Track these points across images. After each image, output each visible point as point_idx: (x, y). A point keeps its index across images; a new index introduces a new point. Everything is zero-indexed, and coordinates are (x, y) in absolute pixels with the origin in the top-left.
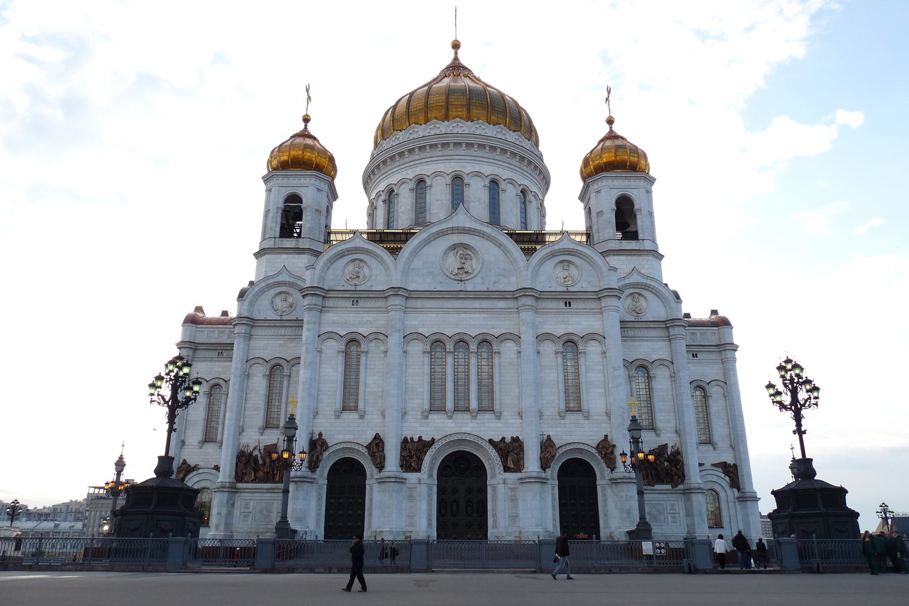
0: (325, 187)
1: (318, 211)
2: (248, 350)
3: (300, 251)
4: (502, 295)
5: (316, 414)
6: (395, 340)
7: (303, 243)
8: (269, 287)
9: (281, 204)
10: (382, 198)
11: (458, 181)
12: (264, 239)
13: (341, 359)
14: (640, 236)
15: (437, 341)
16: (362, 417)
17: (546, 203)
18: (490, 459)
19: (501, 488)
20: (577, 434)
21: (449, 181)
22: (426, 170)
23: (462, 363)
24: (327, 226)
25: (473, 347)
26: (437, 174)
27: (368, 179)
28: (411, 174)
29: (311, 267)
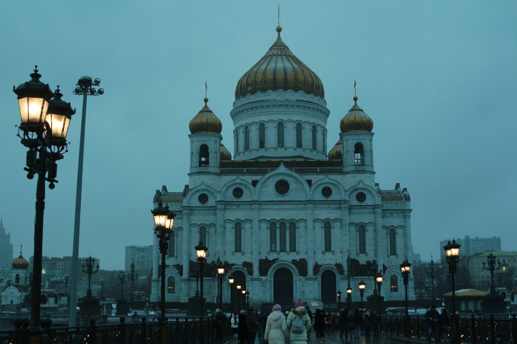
4: (300, 202)
5: (225, 253)
6: (256, 223)
7: (211, 170)
8: (197, 192)
9: (199, 150)
10: (242, 130)
12: (191, 168)
13: (234, 231)
16: (243, 255)
17: (327, 127)
18: (294, 270)
19: (298, 282)
20: (329, 260)
21: (276, 125)
23: (283, 232)
25: (288, 225)
27: (234, 115)
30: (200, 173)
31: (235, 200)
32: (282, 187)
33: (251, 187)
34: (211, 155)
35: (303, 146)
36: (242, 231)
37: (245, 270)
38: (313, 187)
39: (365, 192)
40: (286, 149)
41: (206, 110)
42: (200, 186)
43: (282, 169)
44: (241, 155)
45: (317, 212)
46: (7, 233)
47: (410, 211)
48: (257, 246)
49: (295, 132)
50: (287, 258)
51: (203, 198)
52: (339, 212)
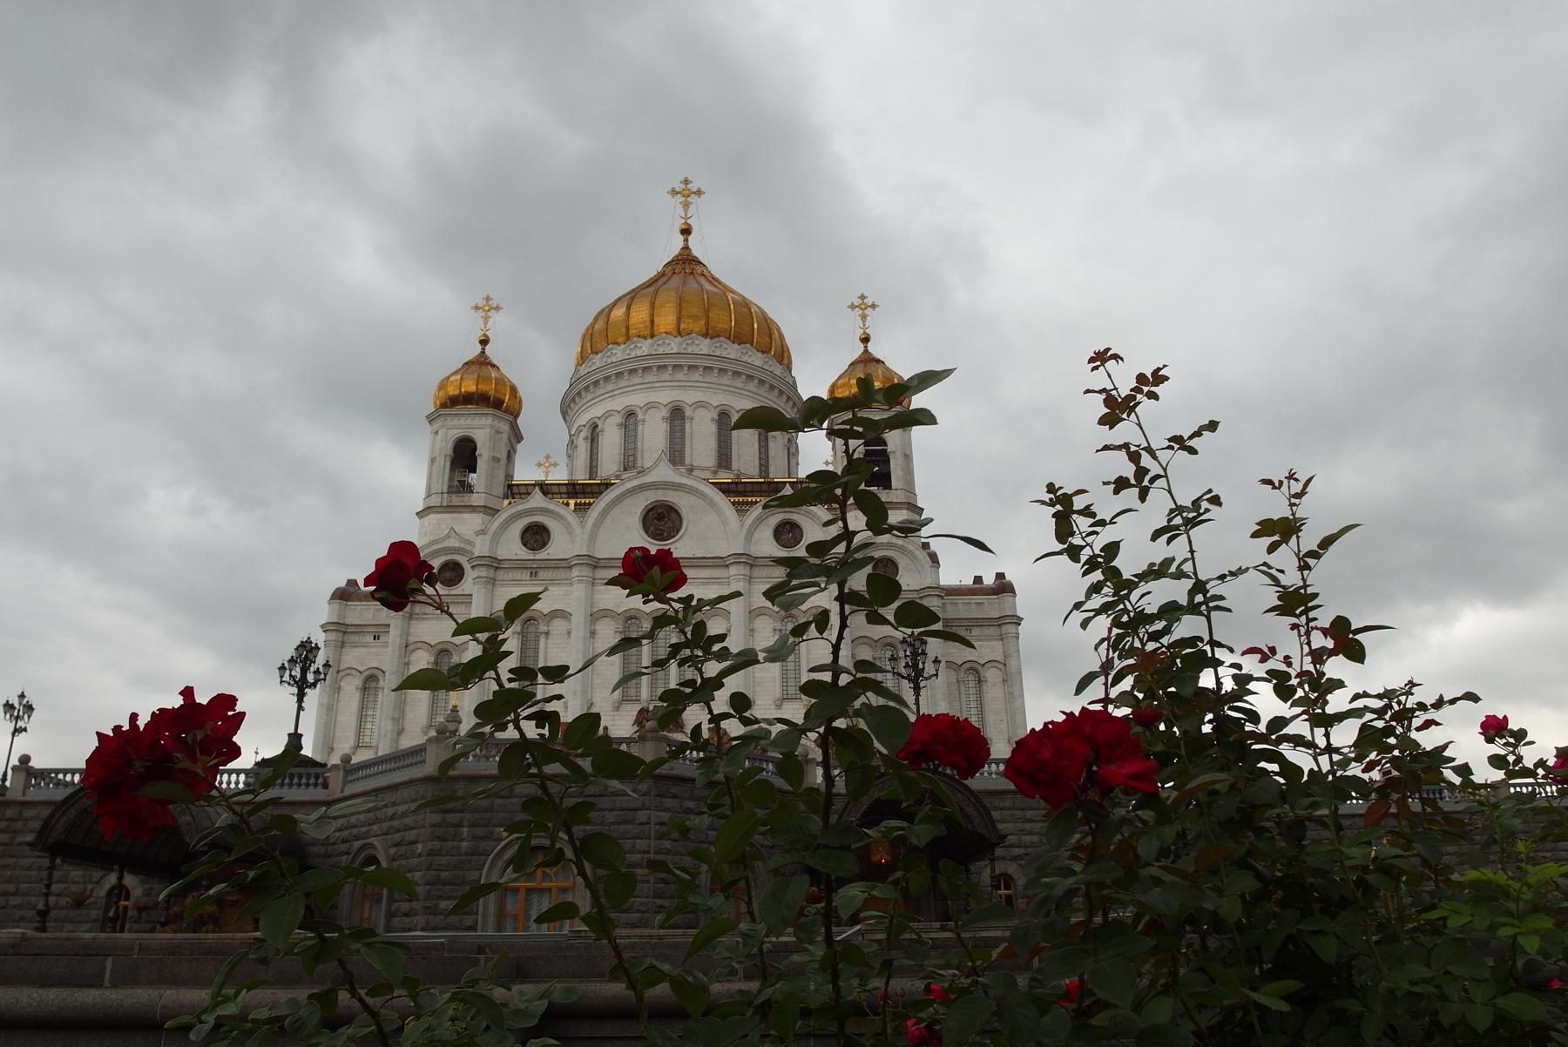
0: (505, 427)
1: (496, 460)
2: (406, 632)
3: (472, 509)
6: (579, 621)
9: (450, 451)
10: (583, 435)
11: (677, 415)
12: (428, 496)
14: (894, 484)
15: (631, 618)
21: (665, 412)
22: (637, 399)
24: (509, 476)
26: (651, 406)
27: (567, 408)
28: (619, 404)
29: (481, 532)
30: (450, 509)
31: (522, 553)
34: (481, 464)
35: (735, 465)
40: (691, 470)
41: (482, 362)
42: (444, 539)
47: (1018, 621)
49: (713, 428)
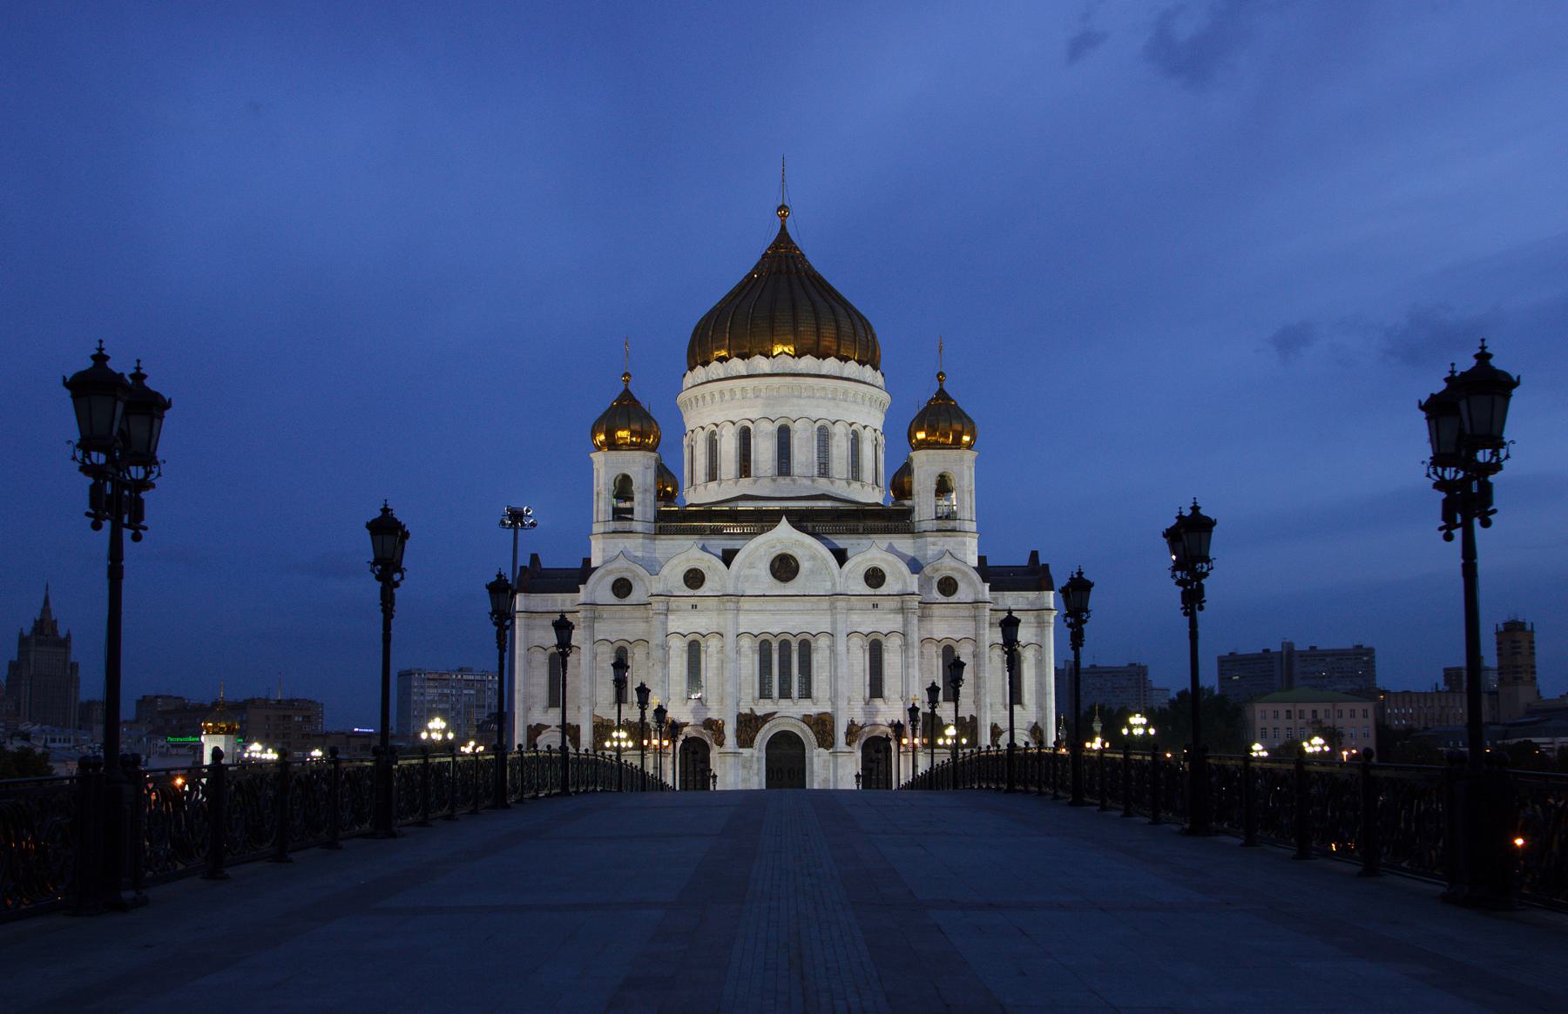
21: (773, 428)
32: (784, 568)
33: (722, 565)
34: (638, 497)
36: (703, 656)
37: (707, 736)
38: (847, 566)
39: (957, 577)
43: (784, 527)
44: (701, 489)
45: (855, 617)
46: (62, 634)
48: (731, 688)
50: (790, 713)
51: (622, 588)
52: (899, 618)
